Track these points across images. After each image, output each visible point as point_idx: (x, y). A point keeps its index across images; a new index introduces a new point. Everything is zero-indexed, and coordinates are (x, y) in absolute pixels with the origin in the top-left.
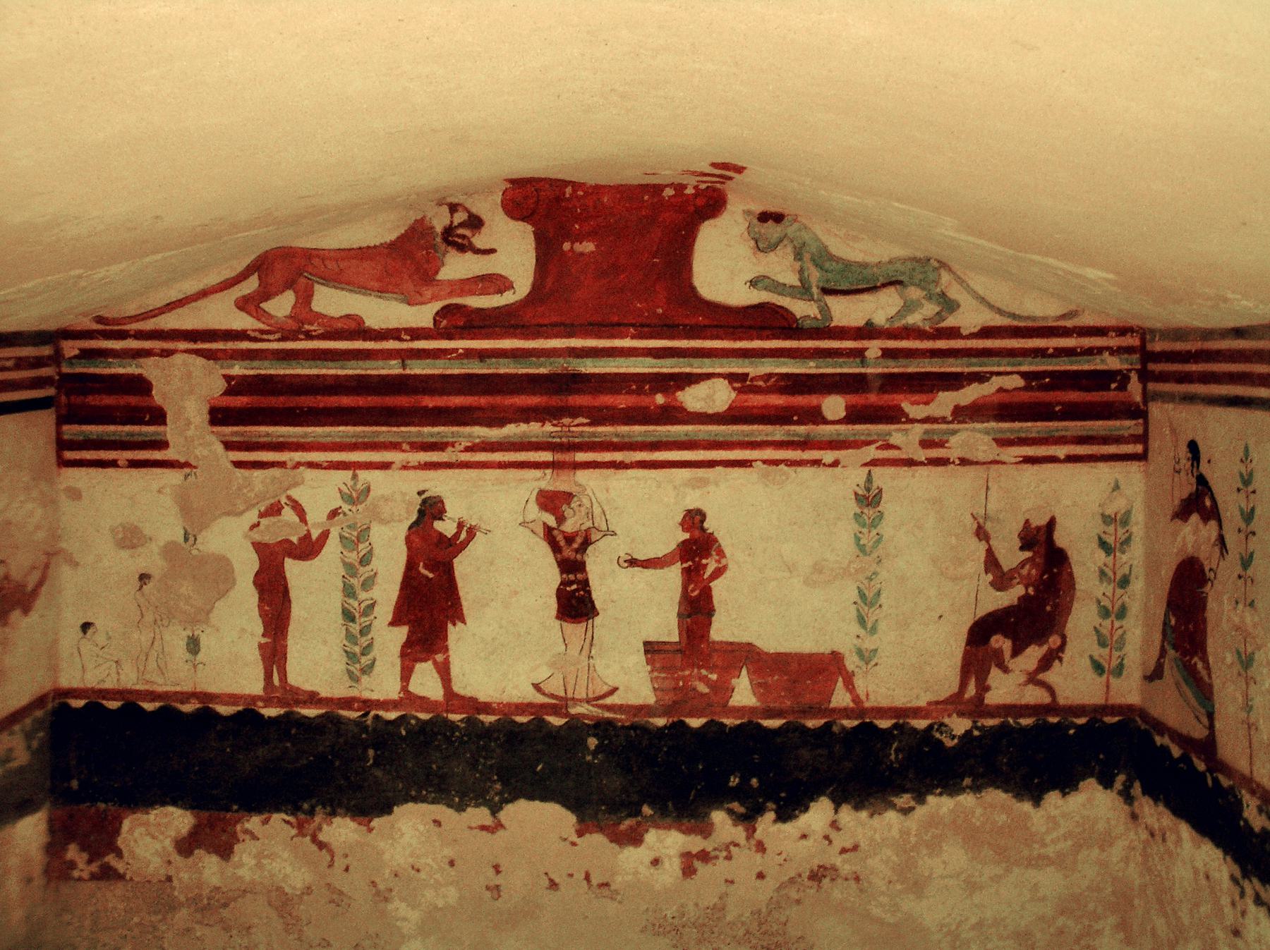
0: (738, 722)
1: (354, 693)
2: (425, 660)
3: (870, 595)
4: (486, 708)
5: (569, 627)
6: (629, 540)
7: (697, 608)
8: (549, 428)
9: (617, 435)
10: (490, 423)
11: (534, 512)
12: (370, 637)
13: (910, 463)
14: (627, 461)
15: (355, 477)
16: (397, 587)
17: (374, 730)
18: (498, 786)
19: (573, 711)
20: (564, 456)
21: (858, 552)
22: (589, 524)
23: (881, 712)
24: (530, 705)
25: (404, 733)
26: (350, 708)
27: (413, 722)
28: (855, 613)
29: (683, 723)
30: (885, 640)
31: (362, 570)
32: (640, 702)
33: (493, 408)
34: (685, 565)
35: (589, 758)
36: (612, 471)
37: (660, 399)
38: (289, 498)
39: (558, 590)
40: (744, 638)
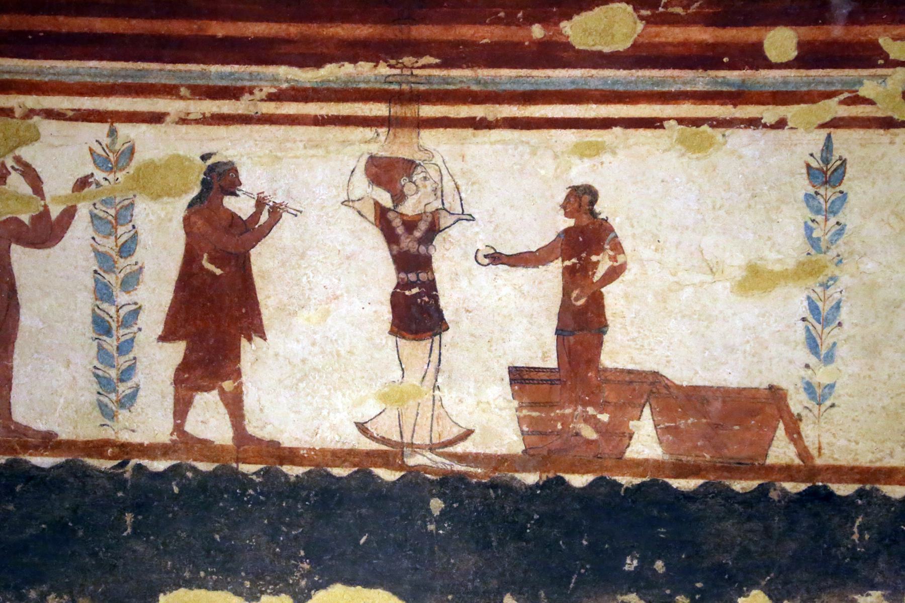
0: (637, 481)
1: (108, 434)
2: (208, 389)
3: (825, 308)
4: (292, 456)
5: (408, 346)
6: (491, 227)
7: (582, 323)
8: (383, 70)
9: (478, 82)
10: (302, 62)
11: (362, 186)
12: (131, 356)
13: (888, 123)
14: (491, 118)
15: (112, 133)
16: (171, 288)
17: (135, 486)
18: (306, 566)
19: (412, 461)
20: (404, 108)
21: (808, 248)
22: (437, 204)
23: (841, 473)
24: (352, 453)
25: (176, 490)
26: (102, 455)
27: (190, 474)
28: (800, 333)
29: (561, 481)
30: (845, 372)
31: (121, 263)
32: (503, 451)
33: (306, 40)
34: (567, 263)
35: (431, 527)
36: (470, 131)
37: (537, 31)
38: (18, 160)
39: (394, 295)
40: (647, 364)
